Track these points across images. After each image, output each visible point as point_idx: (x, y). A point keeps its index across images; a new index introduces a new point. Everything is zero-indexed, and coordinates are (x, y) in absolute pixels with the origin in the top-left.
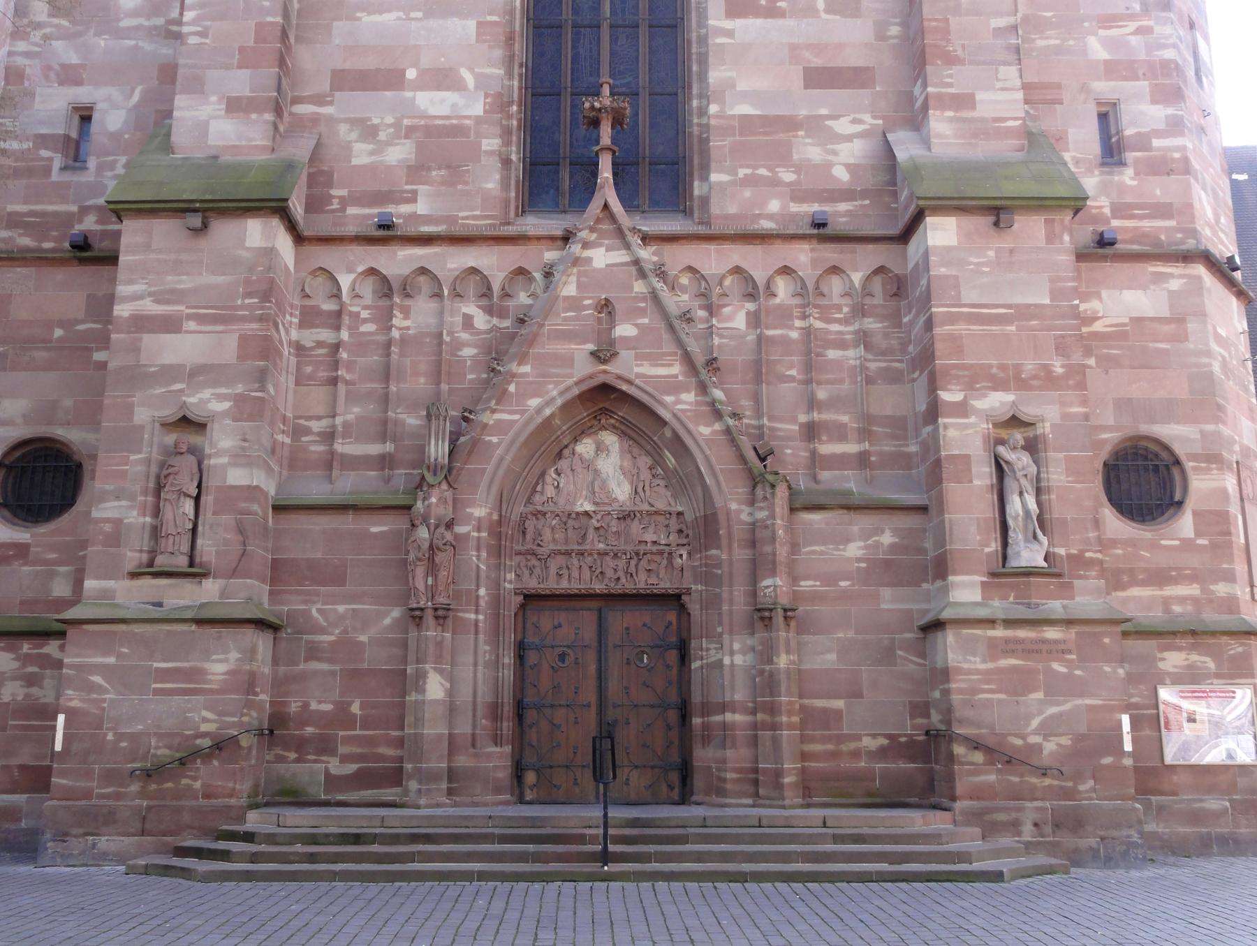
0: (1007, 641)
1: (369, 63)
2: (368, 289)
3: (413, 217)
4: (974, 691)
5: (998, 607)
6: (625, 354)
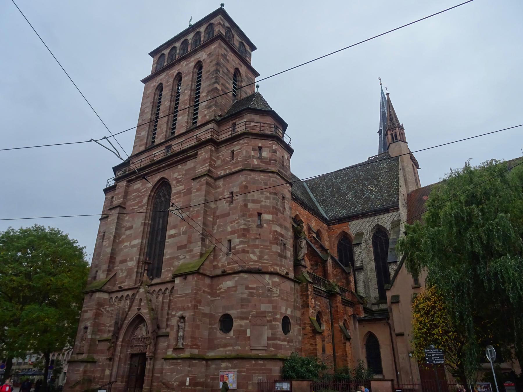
0: (172, 362)
1: (123, 258)
2: (117, 300)
3: (125, 286)
4: (166, 373)
5: (174, 355)
6: (142, 309)
